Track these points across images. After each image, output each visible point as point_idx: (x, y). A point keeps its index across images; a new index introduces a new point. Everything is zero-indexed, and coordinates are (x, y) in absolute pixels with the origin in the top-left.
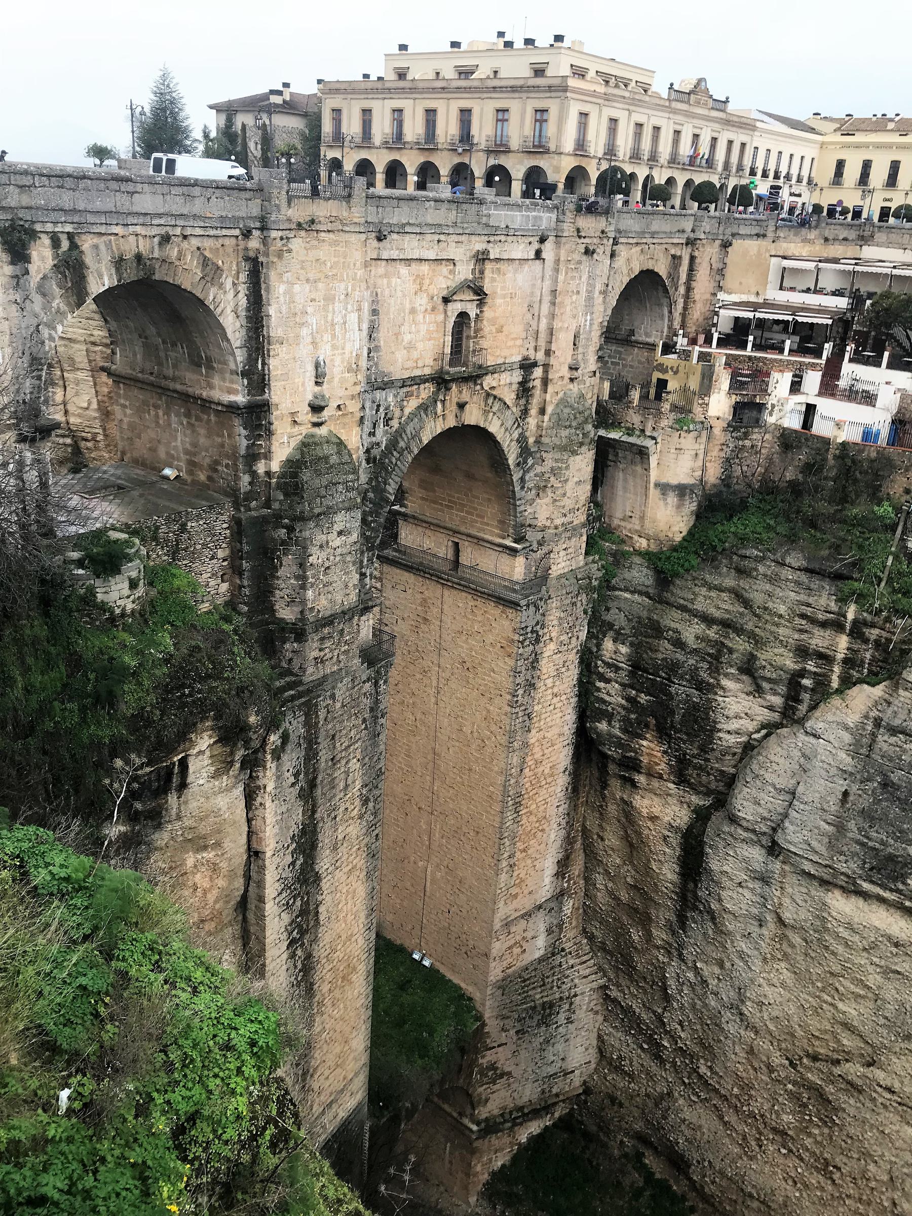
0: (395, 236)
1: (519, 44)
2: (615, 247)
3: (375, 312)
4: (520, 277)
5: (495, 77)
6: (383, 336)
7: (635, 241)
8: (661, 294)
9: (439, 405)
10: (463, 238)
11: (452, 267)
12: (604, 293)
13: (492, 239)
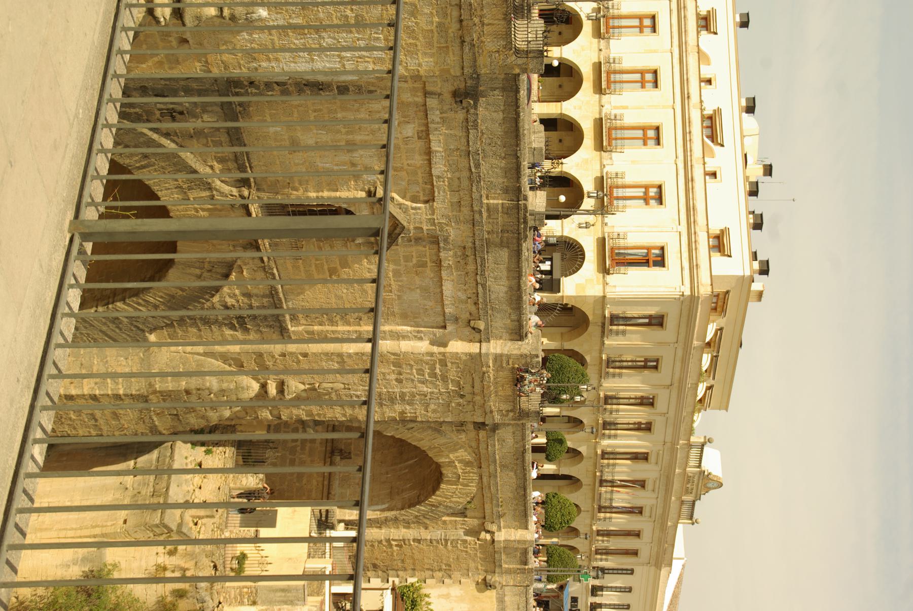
0: (461, 115)
1: (757, 204)
2: (471, 427)
3: (343, 89)
4: (416, 295)
5: (706, 174)
6: (309, 101)
7: (483, 451)
8: (406, 495)
9: (206, 194)
10: (466, 211)
11: (422, 198)
12: (404, 421)
13: (469, 252)
